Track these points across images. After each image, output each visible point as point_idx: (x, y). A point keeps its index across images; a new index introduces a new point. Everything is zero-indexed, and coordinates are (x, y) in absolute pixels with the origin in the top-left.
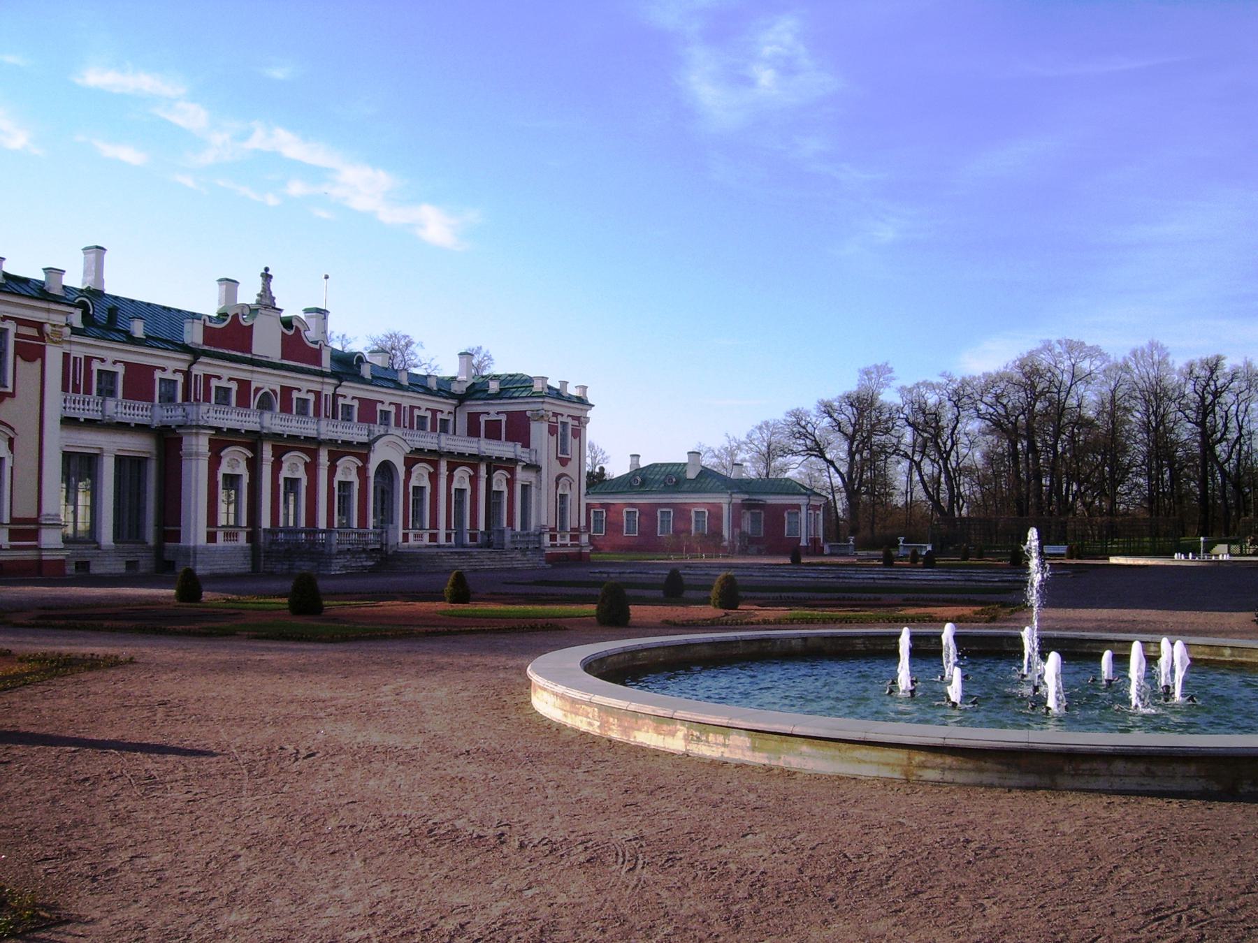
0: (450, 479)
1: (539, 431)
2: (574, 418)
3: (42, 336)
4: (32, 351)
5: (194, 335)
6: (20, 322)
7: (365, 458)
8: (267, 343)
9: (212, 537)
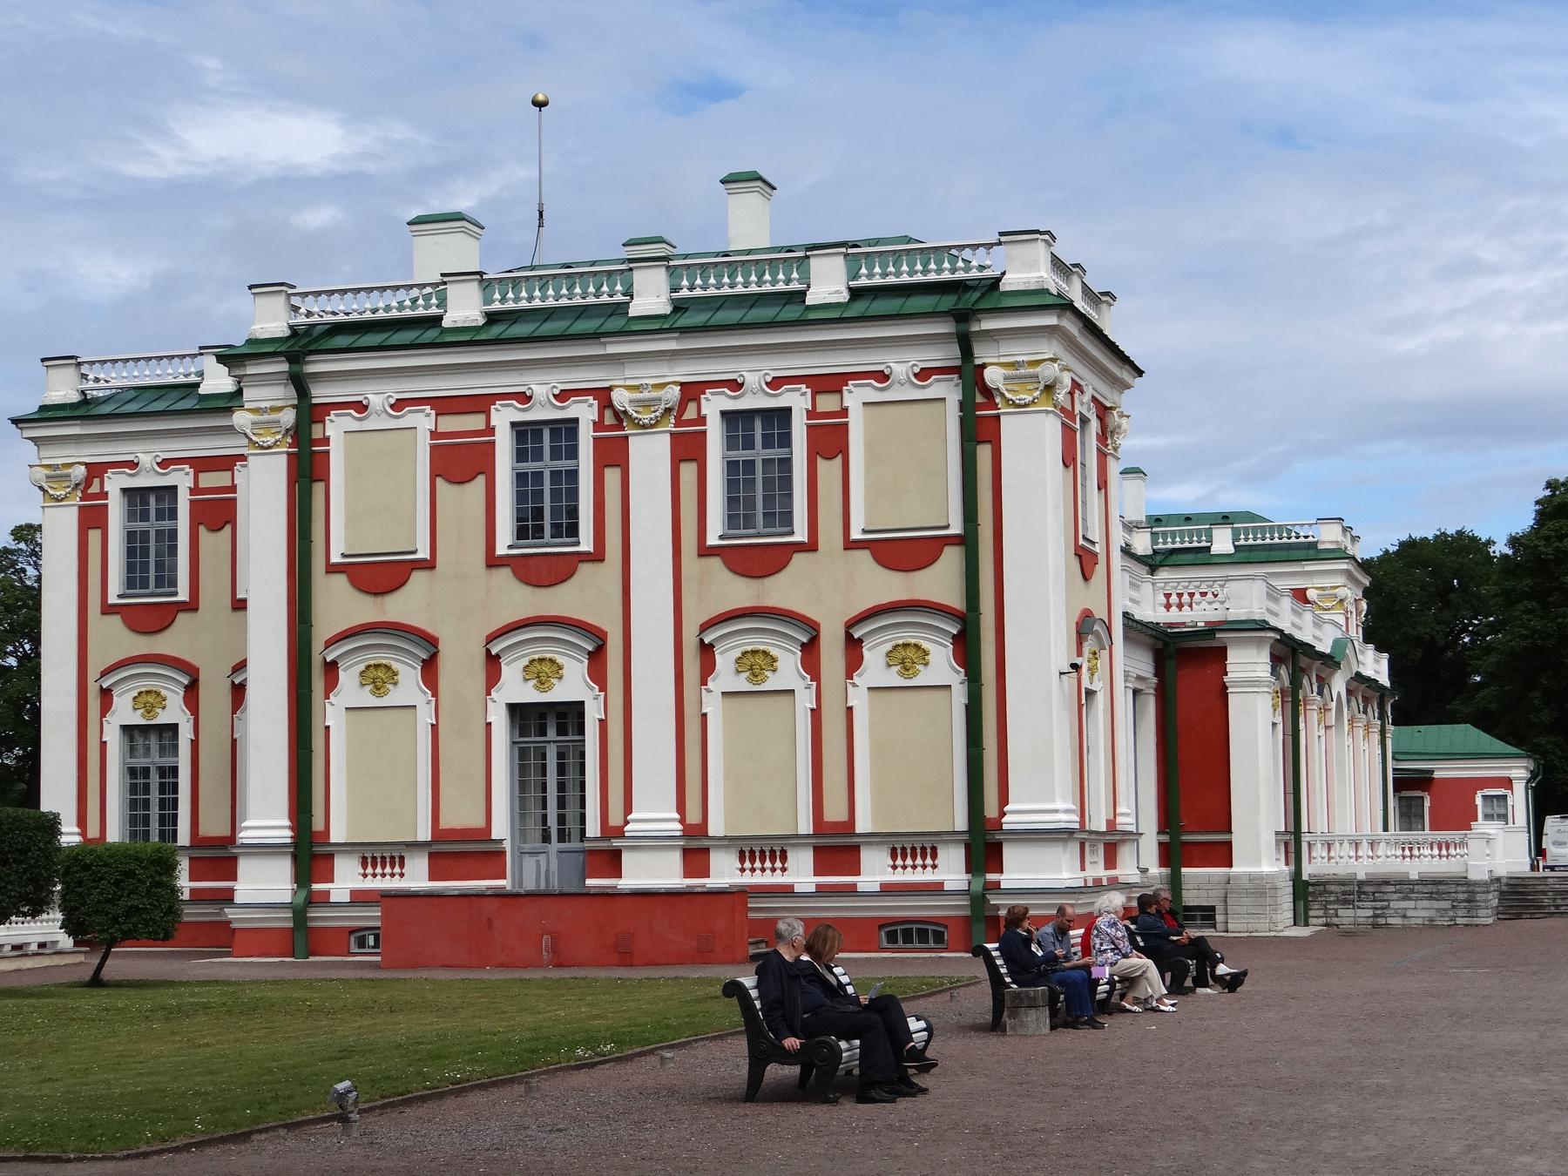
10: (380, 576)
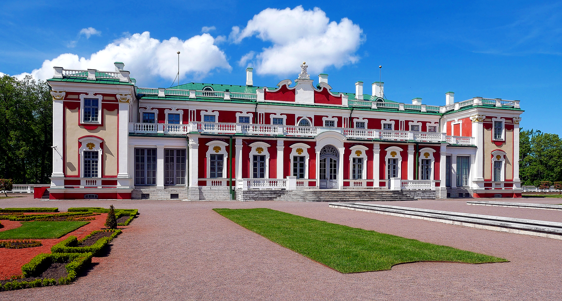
2: (506, 119)
3: (117, 101)
6: (104, 95)
7: (313, 145)
8: (305, 96)
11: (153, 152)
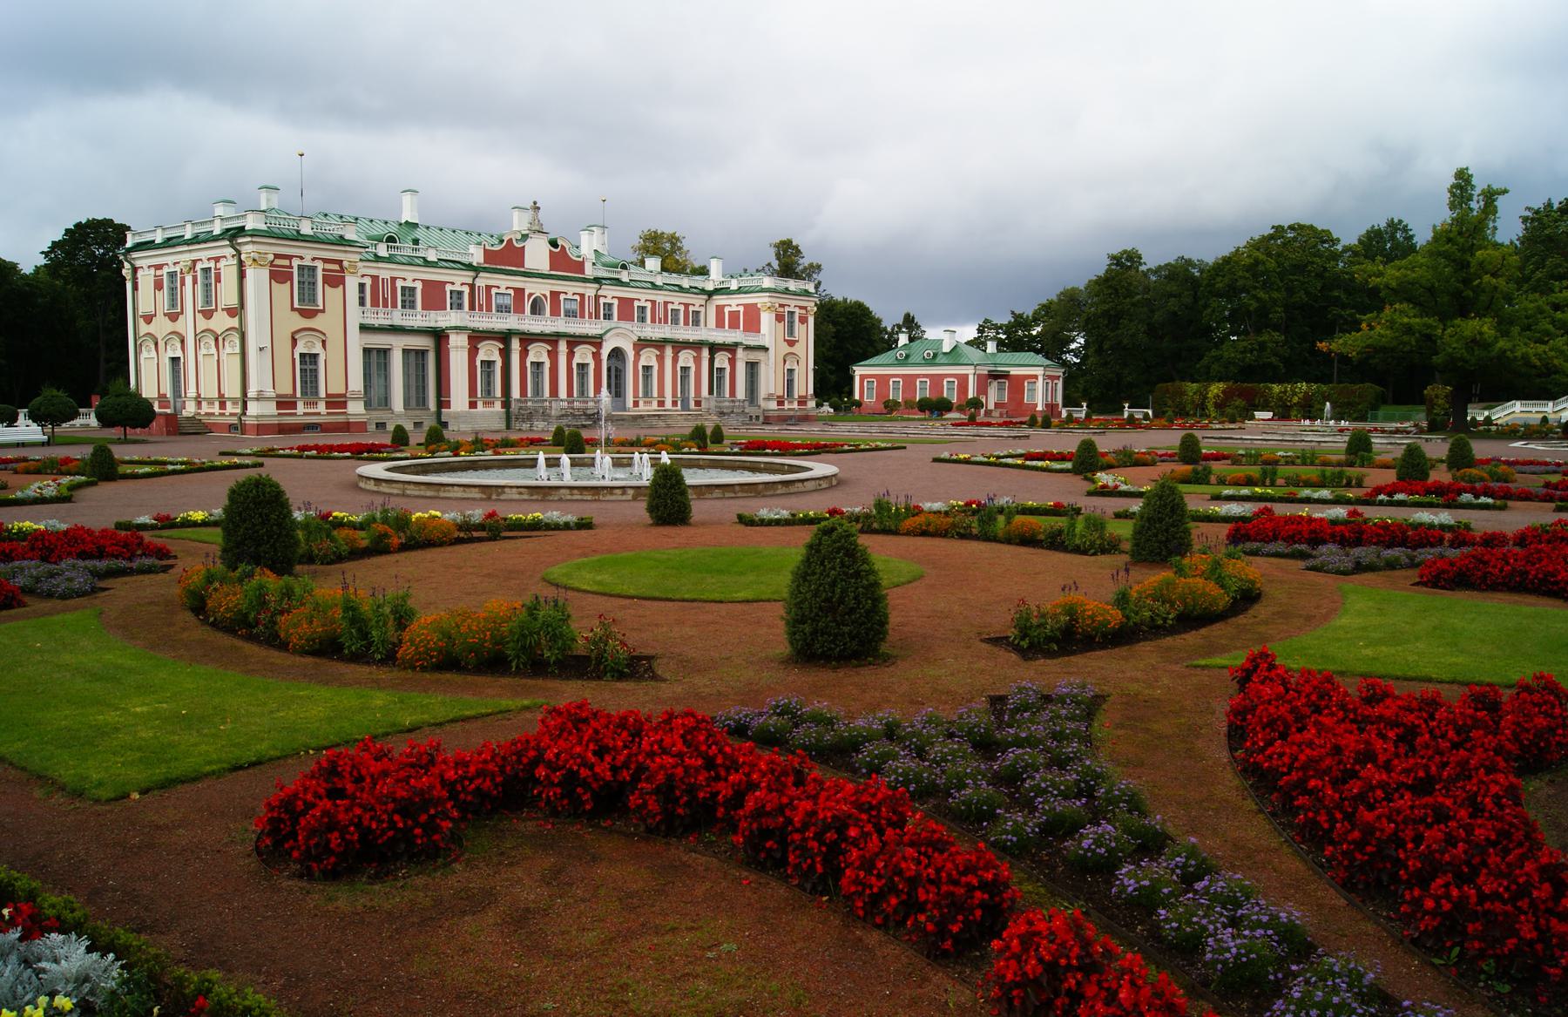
0: (675, 360)
1: (767, 319)
3: (342, 270)
4: (335, 280)
5: (477, 257)
6: (326, 261)
8: (537, 255)
9: (473, 405)
10: (149, 319)
11: (385, 353)
